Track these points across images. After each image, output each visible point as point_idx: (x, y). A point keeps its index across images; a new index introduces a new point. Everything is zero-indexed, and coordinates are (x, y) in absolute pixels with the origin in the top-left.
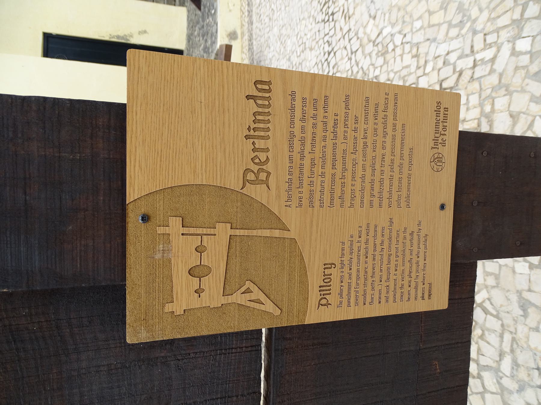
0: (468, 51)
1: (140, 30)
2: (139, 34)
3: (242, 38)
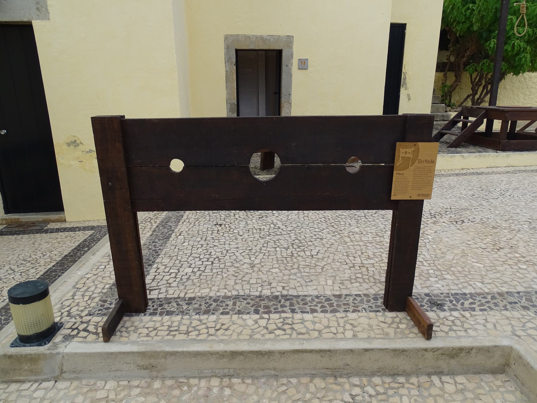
0: (425, 260)
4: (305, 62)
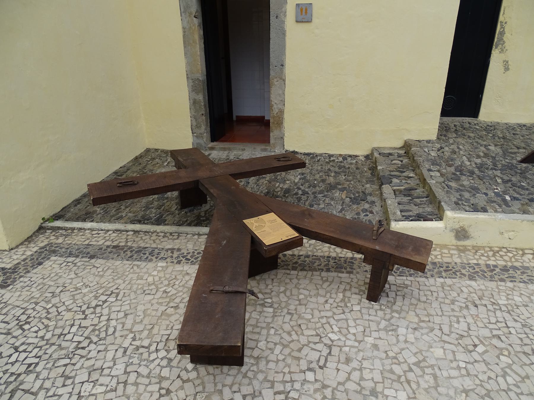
1: (509, 63)
2: (504, 61)
3: (458, 248)
4: (306, 10)
